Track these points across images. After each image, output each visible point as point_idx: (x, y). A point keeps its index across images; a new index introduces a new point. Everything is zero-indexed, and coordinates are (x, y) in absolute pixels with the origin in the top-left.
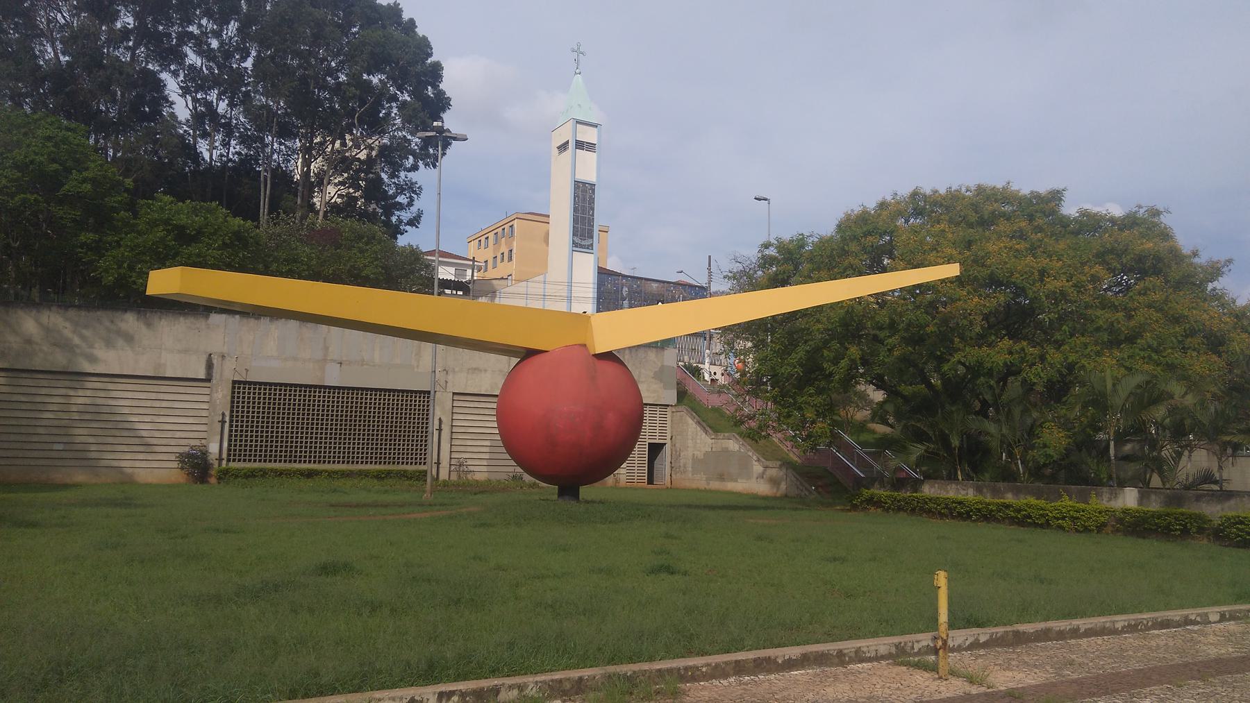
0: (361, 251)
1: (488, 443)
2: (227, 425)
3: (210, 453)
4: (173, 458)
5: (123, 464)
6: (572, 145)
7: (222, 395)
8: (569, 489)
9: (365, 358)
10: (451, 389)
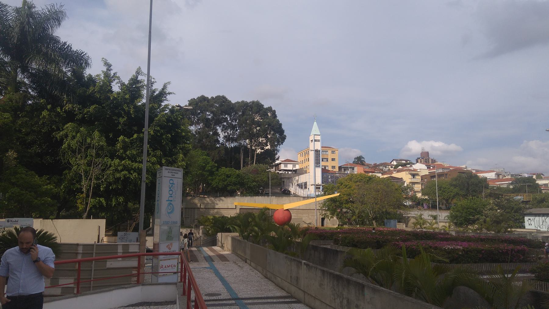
0: (263, 175)
6: (313, 141)
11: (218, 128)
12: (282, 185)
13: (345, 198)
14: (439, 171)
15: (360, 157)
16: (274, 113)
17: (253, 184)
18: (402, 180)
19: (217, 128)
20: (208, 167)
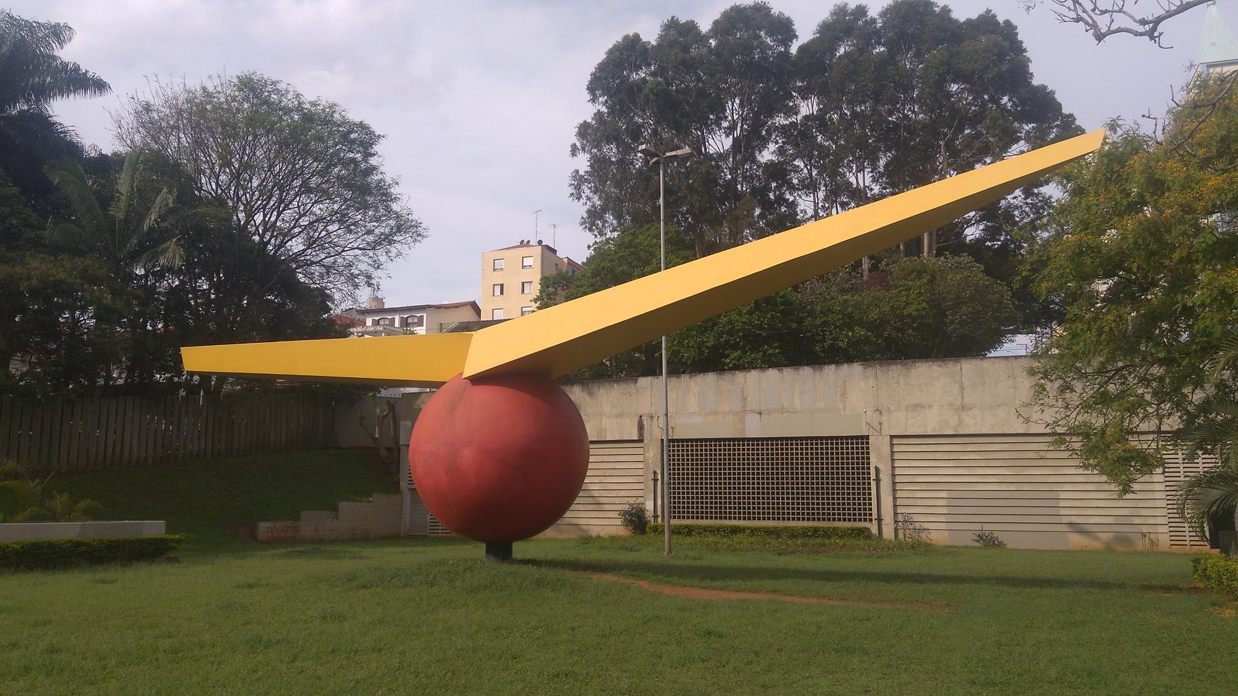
2: (659, 483)
3: (647, 511)
5: (581, 522)
7: (652, 453)
8: (500, 550)
9: (785, 405)
10: (887, 431)
17: (847, 336)
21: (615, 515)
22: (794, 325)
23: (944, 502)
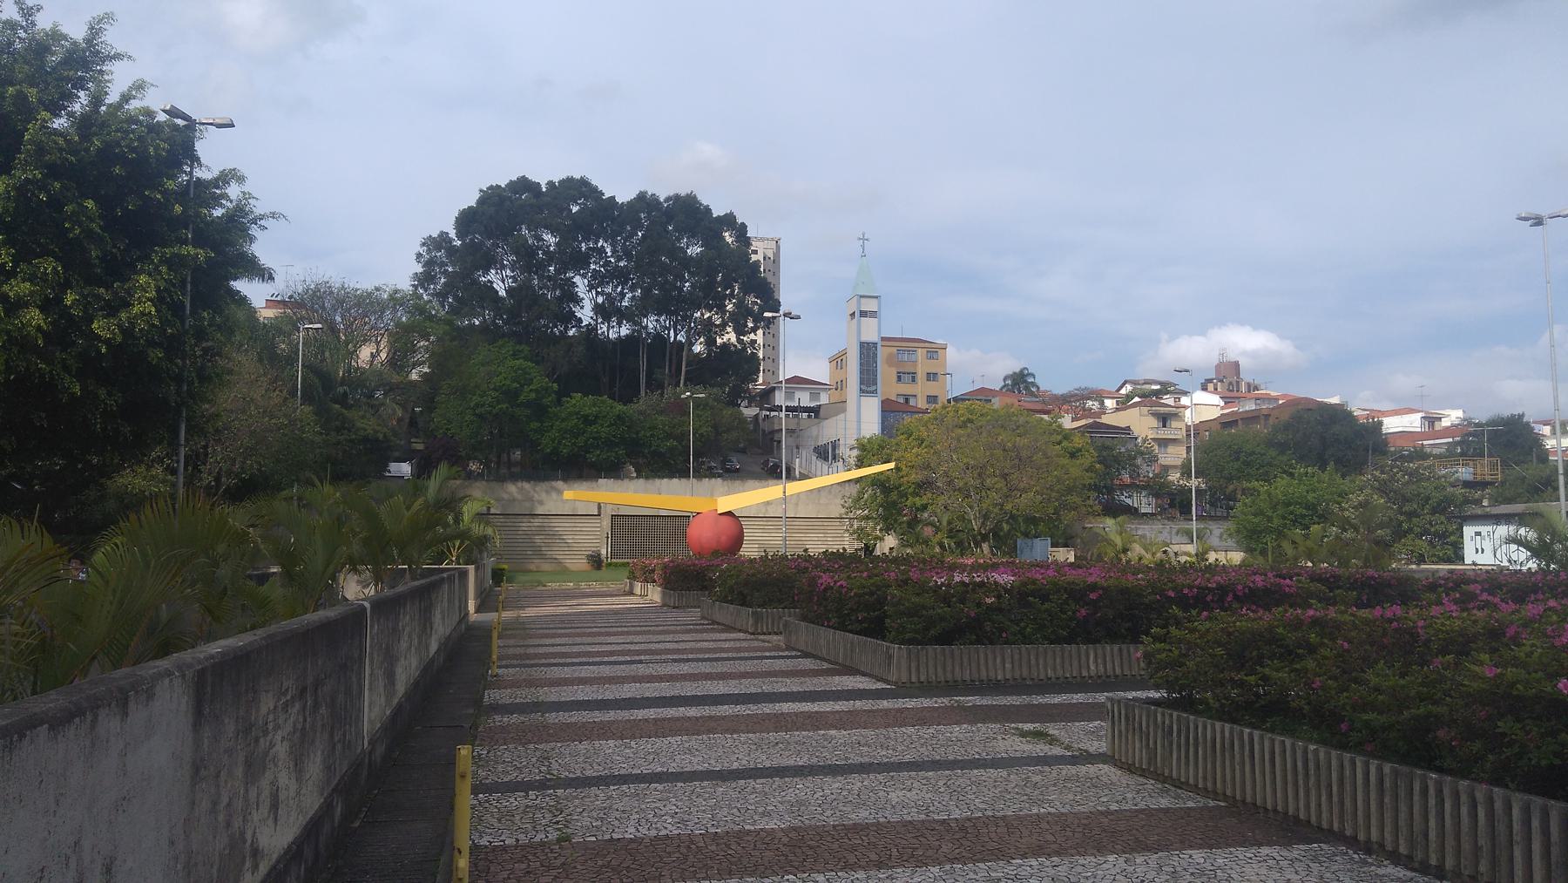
1: (757, 546)
4: (583, 557)
11: (577, 279)
12: (775, 452)
13: (915, 477)
14: (1247, 408)
15: (1022, 371)
16: (741, 231)
18: (1129, 434)
19: (574, 280)
20: (527, 395)
21: (583, 557)
22: (635, 436)
23: (756, 550)
